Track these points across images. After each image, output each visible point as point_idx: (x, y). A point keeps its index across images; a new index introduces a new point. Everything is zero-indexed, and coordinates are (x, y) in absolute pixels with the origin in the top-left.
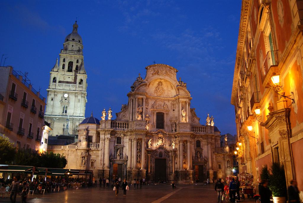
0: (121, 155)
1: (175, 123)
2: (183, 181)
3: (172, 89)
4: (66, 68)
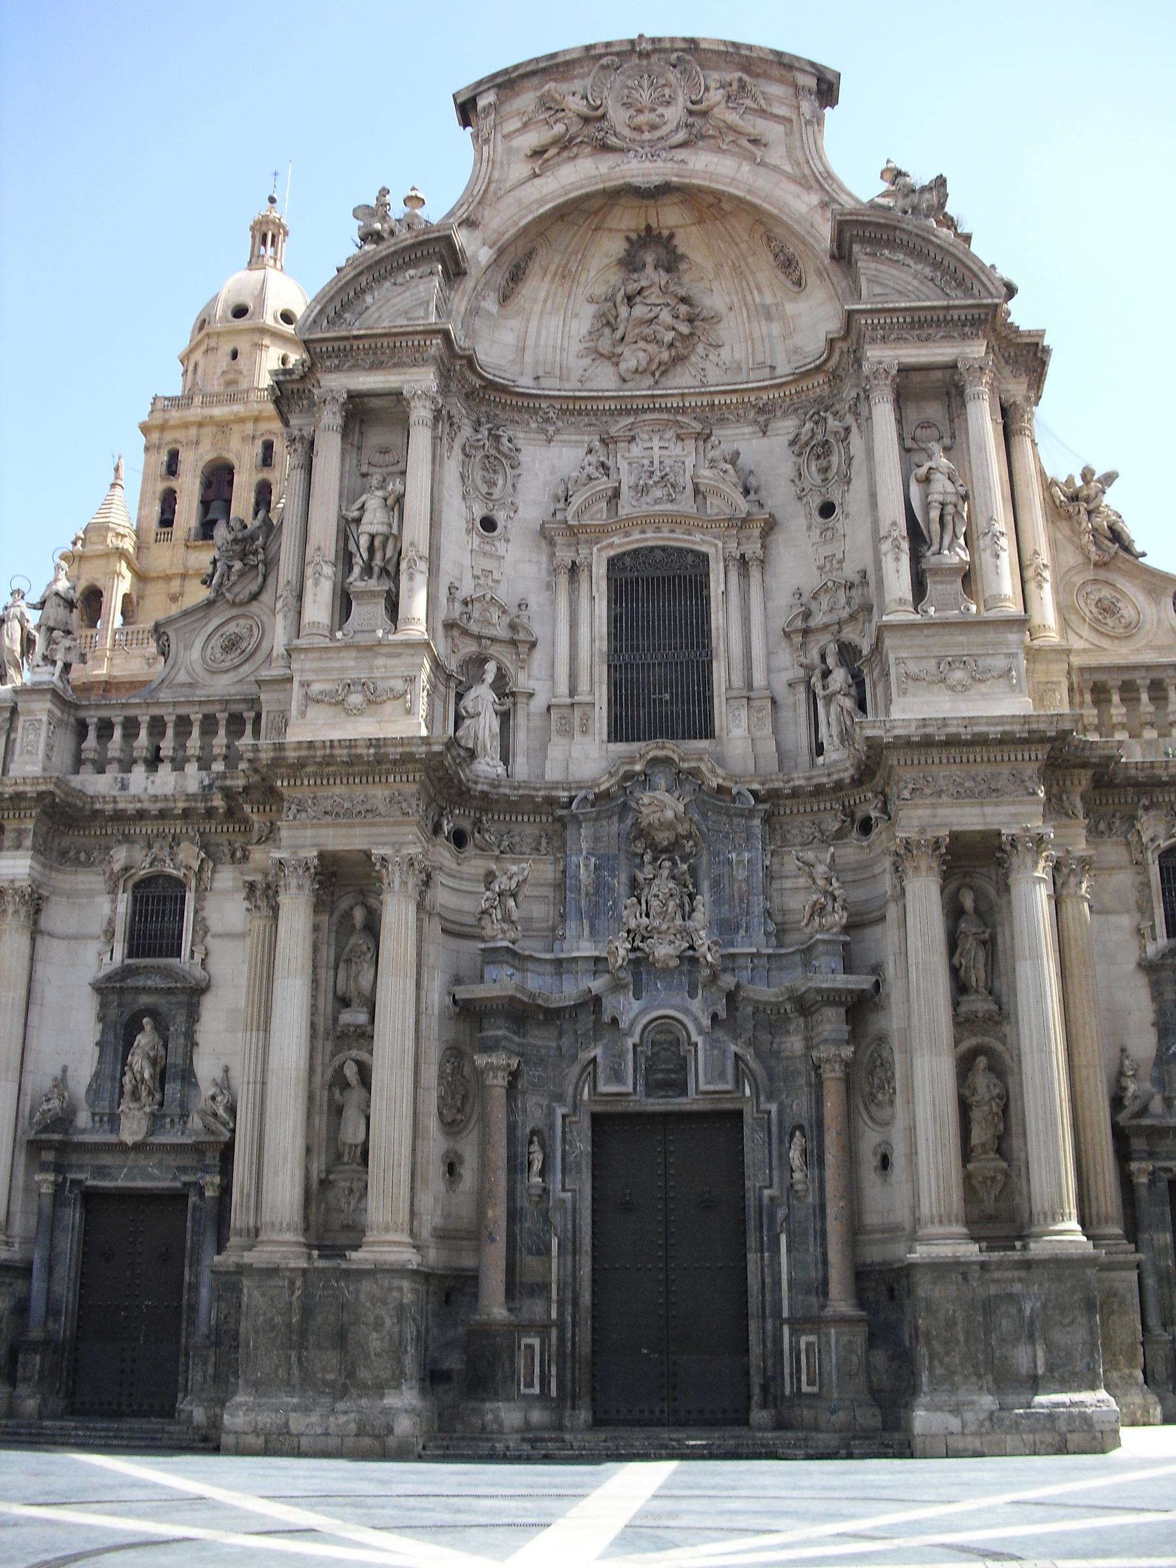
0: (173, 1089)
1: (847, 652)
2: (956, 1410)
3: (798, 283)
4: (188, 513)
